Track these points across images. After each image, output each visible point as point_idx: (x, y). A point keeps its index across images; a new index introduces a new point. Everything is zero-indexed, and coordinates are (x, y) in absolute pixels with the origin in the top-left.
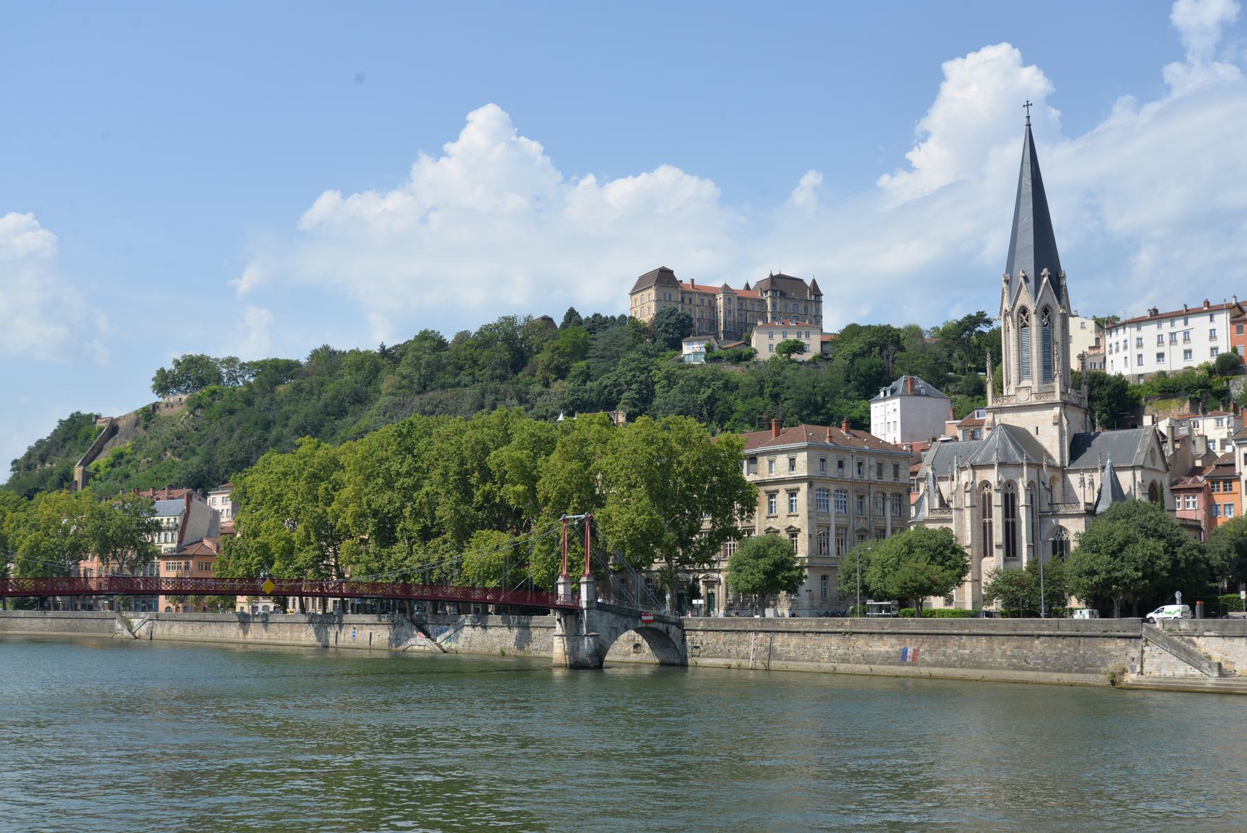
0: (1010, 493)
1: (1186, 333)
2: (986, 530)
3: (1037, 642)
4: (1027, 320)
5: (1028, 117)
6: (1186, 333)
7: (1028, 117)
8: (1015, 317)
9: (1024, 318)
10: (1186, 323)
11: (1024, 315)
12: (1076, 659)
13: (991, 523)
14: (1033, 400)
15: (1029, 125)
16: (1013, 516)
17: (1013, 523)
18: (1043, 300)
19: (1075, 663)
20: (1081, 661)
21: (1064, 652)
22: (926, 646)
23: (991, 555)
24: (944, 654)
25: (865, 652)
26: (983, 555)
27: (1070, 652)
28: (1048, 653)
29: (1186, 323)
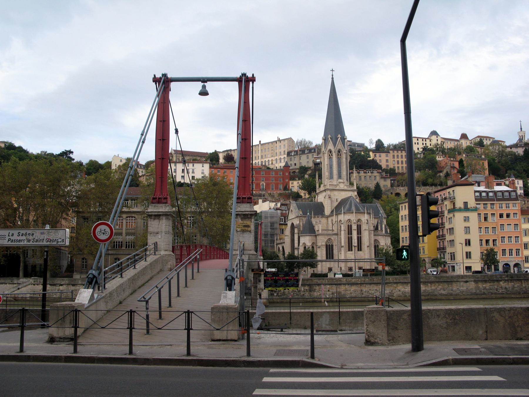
0: (350, 224)
1: (193, 170)
2: (350, 240)
3: (501, 283)
4: (340, 155)
5: (332, 75)
6: (193, 170)
7: (332, 75)
8: (336, 153)
9: (339, 154)
10: (193, 166)
11: (331, 153)
12: (521, 289)
13: (351, 237)
14: (346, 188)
15: (333, 78)
16: (360, 234)
17: (360, 237)
18: (338, 147)
19: (522, 290)
20: (524, 289)
21: (515, 286)
22: (440, 287)
23: (352, 250)
24: (452, 290)
25: (403, 291)
26: (348, 250)
27: (518, 286)
28: (507, 287)
29: (193, 166)
